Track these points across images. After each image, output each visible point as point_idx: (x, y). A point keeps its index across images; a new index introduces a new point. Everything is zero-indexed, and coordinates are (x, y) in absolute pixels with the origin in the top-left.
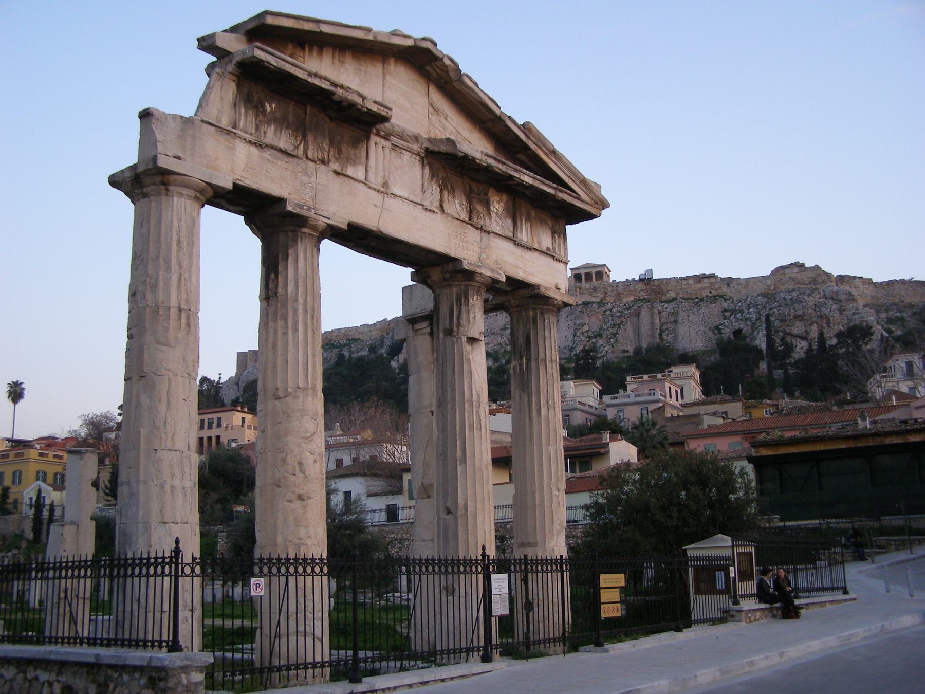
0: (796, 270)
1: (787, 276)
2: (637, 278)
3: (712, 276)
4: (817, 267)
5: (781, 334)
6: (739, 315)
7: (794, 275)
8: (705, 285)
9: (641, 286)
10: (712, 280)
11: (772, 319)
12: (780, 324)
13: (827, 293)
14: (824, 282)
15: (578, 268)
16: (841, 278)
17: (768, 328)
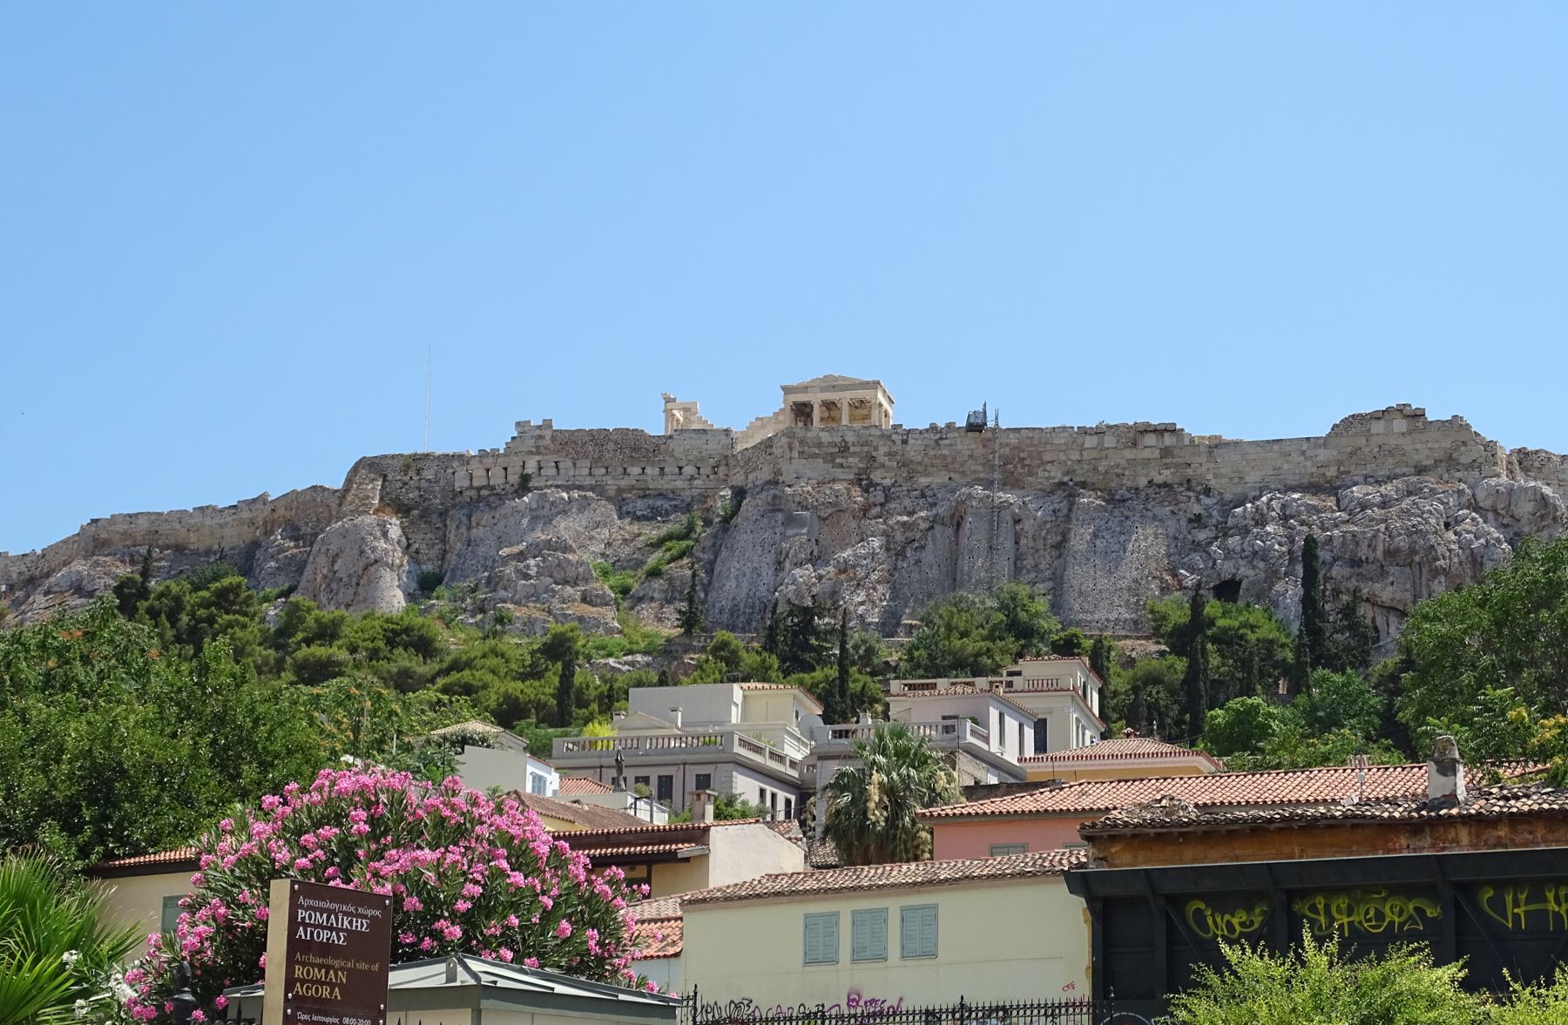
0: (1400, 425)
1: (1375, 441)
3: (1171, 430)
4: (1456, 425)
5: (1345, 598)
6: (1234, 541)
7: (1393, 442)
8: (1146, 454)
9: (969, 444)
10: (1168, 440)
11: (1324, 555)
12: (1347, 571)
13: (1481, 495)
14: (1473, 465)
15: (804, 388)
16: (1525, 460)
17: (1309, 581)
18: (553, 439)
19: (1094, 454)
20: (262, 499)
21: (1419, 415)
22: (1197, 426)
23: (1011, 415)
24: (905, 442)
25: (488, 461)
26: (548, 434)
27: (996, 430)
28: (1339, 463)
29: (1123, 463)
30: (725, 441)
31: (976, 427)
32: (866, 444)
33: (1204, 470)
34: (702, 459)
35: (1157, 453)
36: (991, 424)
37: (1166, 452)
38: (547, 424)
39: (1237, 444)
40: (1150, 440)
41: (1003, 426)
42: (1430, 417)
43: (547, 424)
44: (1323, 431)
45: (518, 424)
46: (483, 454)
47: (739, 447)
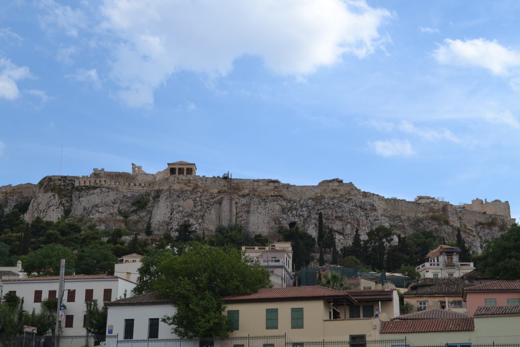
0: (336, 184)
1: (330, 188)
2: (221, 176)
3: (276, 182)
7: (335, 188)
8: (271, 187)
9: (223, 182)
10: (276, 184)
16: (365, 195)
18: (104, 174)
19: (257, 187)
20: (10, 186)
21: (341, 182)
22: (284, 181)
23: (235, 175)
24: (206, 181)
25: (85, 179)
26: (103, 172)
27: (231, 179)
28: (321, 193)
29: (265, 190)
30: (153, 177)
31: (226, 178)
32: (195, 180)
33: (284, 192)
34: (146, 182)
35: (273, 188)
36: (230, 177)
37: (276, 187)
38: (103, 170)
39: (294, 186)
40: (271, 184)
41: (233, 178)
42: (344, 182)
43: (103, 170)
44: (316, 184)
45: (94, 169)
46: (83, 177)
47: (157, 180)
